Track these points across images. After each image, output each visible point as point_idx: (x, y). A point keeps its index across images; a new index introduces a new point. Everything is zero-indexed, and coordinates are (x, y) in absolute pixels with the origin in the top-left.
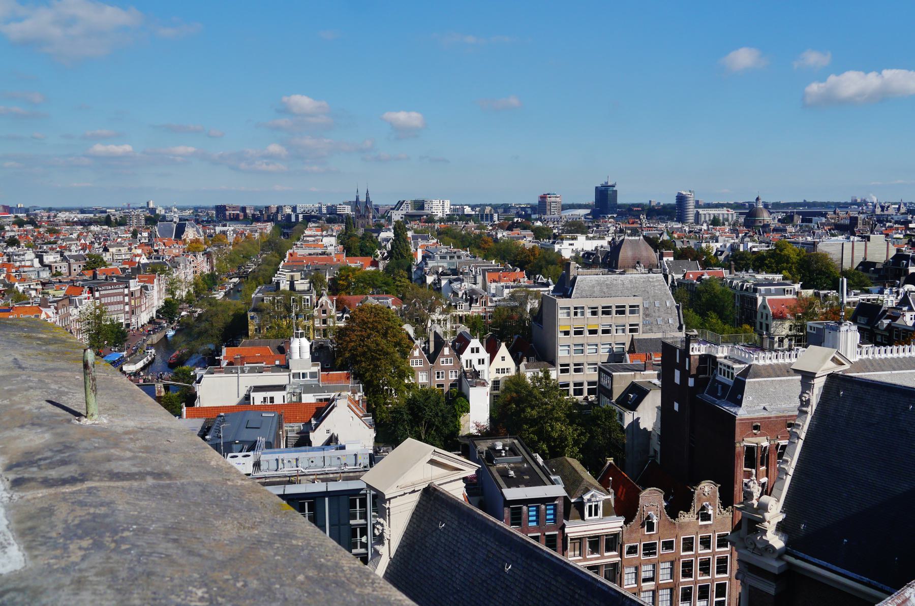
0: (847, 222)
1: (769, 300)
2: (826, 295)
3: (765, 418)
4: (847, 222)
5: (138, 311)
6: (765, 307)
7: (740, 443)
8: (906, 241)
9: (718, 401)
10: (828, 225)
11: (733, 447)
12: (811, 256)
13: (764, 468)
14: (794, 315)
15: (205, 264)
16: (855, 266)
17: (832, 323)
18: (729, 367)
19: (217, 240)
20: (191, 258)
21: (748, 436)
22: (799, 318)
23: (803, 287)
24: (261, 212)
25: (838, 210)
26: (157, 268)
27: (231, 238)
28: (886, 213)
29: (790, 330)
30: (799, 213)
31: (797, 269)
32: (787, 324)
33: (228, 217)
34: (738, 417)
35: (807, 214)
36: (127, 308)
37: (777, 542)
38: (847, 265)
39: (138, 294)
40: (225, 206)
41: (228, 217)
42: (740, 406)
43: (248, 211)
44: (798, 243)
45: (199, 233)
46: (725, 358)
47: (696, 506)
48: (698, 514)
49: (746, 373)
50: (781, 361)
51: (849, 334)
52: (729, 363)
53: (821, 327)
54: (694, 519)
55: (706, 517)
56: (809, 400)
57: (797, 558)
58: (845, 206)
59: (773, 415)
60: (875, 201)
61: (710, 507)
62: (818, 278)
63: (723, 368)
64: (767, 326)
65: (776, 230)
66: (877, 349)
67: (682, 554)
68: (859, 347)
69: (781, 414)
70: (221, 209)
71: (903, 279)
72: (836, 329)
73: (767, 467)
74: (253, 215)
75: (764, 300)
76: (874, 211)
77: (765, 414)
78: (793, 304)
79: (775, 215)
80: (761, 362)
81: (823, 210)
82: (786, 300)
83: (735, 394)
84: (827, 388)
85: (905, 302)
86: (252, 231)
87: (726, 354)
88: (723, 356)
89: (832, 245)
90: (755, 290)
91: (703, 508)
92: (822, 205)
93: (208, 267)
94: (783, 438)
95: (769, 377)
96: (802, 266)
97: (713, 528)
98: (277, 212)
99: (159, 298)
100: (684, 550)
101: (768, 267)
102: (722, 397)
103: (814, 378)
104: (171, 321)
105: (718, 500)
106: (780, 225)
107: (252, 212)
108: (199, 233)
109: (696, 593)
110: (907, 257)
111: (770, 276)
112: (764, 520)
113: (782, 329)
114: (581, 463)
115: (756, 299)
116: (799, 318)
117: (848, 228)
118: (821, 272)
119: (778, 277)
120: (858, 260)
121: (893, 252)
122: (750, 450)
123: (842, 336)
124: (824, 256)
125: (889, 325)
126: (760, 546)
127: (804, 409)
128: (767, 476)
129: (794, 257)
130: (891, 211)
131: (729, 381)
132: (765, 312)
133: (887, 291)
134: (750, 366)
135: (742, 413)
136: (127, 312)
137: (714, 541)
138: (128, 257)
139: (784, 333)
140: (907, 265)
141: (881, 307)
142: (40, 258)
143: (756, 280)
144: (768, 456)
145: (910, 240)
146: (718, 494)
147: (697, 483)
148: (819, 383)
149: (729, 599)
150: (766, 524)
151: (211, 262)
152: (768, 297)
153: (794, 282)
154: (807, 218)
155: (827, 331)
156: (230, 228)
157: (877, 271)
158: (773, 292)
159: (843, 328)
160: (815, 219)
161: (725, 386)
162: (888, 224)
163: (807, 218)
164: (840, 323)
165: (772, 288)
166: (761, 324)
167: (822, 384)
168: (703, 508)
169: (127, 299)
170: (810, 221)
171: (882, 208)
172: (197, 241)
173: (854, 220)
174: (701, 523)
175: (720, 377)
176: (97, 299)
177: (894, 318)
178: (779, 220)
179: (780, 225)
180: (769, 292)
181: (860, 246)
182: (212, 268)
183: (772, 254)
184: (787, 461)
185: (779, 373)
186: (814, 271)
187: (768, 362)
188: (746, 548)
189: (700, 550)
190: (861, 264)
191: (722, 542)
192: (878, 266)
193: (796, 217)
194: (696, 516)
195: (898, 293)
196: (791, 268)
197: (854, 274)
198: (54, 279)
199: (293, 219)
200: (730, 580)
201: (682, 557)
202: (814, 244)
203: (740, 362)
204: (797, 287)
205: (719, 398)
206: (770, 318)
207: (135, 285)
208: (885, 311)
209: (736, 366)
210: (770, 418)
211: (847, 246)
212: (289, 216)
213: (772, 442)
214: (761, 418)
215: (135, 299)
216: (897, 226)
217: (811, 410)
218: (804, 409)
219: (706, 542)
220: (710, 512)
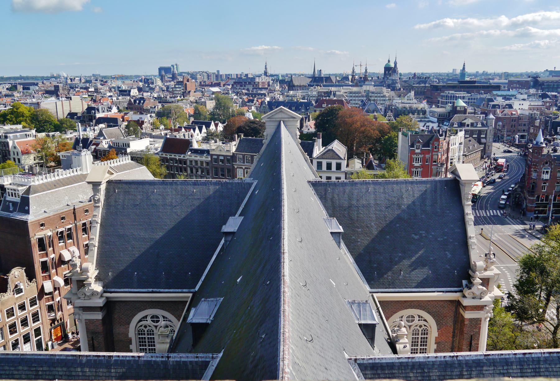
0: (53, 89)
1: (17, 142)
2: (53, 136)
3: (46, 218)
4: (53, 89)
6: (15, 148)
7: (33, 237)
8: (90, 99)
9: (11, 214)
10: (41, 91)
11: (30, 242)
12: (37, 112)
13: (51, 248)
14: (36, 150)
16: (65, 116)
17: (75, 152)
18: (15, 190)
21: (38, 232)
22: (39, 152)
23: (38, 131)
25: (45, 82)
28: (73, 82)
29: (35, 160)
30: (20, 84)
31: (31, 121)
32: (32, 157)
34: (29, 222)
35: (27, 85)
37: (98, 288)
38: (61, 116)
42: (29, 213)
44: (27, 104)
46: (11, 184)
47: (11, 286)
48: (13, 291)
49: (28, 191)
50: (49, 180)
51: (87, 156)
52: (15, 187)
53: (69, 155)
54: (12, 295)
55: (19, 291)
56: (99, 199)
57: (111, 292)
58: (48, 79)
59: (51, 214)
60: (66, 76)
61: (21, 284)
62: (44, 125)
63: (10, 191)
64: (19, 159)
65: (6, 96)
66: (103, 163)
67: (7, 320)
68: (93, 163)
69: (56, 213)
71: (94, 121)
72: (79, 155)
73: (53, 247)
75: (14, 142)
76: (67, 82)
77: (46, 215)
78: (34, 143)
79: (3, 85)
80: (37, 183)
81: (36, 82)
82: (29, 141)
83: (24, 205)
84: (107, 189)
85: (101, 134)
87: (10, 182)
88: (9, 183)
89: (49, 104)
90: (6, 137)
91: (16, 286)
92: (32, 78)
94: (60, 227)
95: (44, 191)
96: (33, 118)
97: (26, 296)
100: (8, 318)
101: (10, 121)
102: (14, 210)
103: (100, 185)
105: (25, 278)
106: (10, 93)
109: (21, 340)
110: (94, 108)
111: (14, 127)
112: (88, 278)
113: (29, 161)
114: (359, 260)
115: (8, 143)
116: (39, 152)
117: (54, 92)
118: (46, 121)
119: (19, 127)
120: (67, 112)
121: (86, 107)
122: (41, 241)
123: (83, 158)
124: (46, 111)
125: (95, 149)
126: (88, 294)
127: (97, 205)
128: (54, 253)
129: (27, 113)
130: (77, 81)
131: (18, 200)
132: (15, 151)
133: (88, 129)
134: (30, 187)
135: (31, 218)
137: (28, 305)
139: (30, 163)
140: (95, 113)
141: (89, 139)
143: (5, 130)
144: (52, 241)
145: (92, 99)
146: (25, 274)
147: (9, 271)
148: (103, 187)
149: (44, 335)
150: (90, 280)
152: (16, 141)
153: (31, 129)
154: (26, 87)
155: (73, 157)
157: (79, 118)
158: (19, 137)
159: (83, 154)
160: (31, 87)
161: (14, 204)
162: (77, 89)
163: (26, 87)
164: (81, 151)
165: (18, 134)
166: (14, 159)
167: (105, 188)
168: (16, 286)
170: (29, 89)
171: (71, 79)
173: (57, 87)
174: (16, 296)
175: (9, 198)
177: (97, 145)
178: (7, 89)
179: (10, 93)
180: (16, 137)
181: (66, 103)
183: (12, 112)
184: (93, 239)
185: (49, 187)
186: (40, 122)
187: (41, 182)
188: (79, 298)
189: (19, 314)
190: (69, 114)
191: (33, 302)
192: (79, 115)
193: (18, 86)
194: (12, 293)
195: (94, 129)
196: (26, 120)
197: (66, 121)
200: (42, 324)
201: (8, 322)
202: (38, 104)
203: (22, 185)
204: (34, 131)
205: (11, 212)
206: (20, 154)
208: (91, 141)
209: (20, 188)
210: (50, 217)
211: (59, 103)
213: (54, 232)
214: (44, 218)
216: (82, 90)
217: (101, 204)
218: (97, 205)
219: (22, 307)
220: (22, 287)
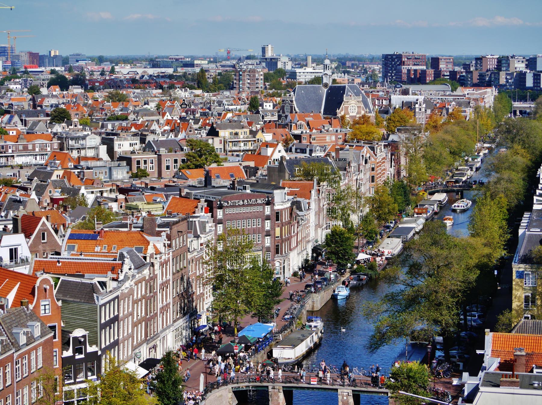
5: (285, 247)
15: (387, 165)
19: (396, 119)
20: (366, 151)
24: (466, 67)
26: (312, 171)
27: (421, 117)
33: (405, 78)
36: (268, 242)
39: (285, 217)
40: (399, 57)
41: (405, 78)
43: (442, 66)
45: (366, 105)
70: (392, 63)
74: (453, 74)
86: (459, 104)
93: (392, 170)
98: (499, 68)
99: (318, 226)
104: (341, 270)
107: (450, 67)
108: (366, 105)
136: (268, 250)
138: (249, 146)
142: (108, 142)
151: (398, 162)
156: (418, 95)
169: (268, 225)
172: (364, 120)
176: (220, 222)
182: (398, 173)
198: (137, 183)
199: (529, 83)
207: (281, 200)
212: (522, 76)
215: (282, 225)
